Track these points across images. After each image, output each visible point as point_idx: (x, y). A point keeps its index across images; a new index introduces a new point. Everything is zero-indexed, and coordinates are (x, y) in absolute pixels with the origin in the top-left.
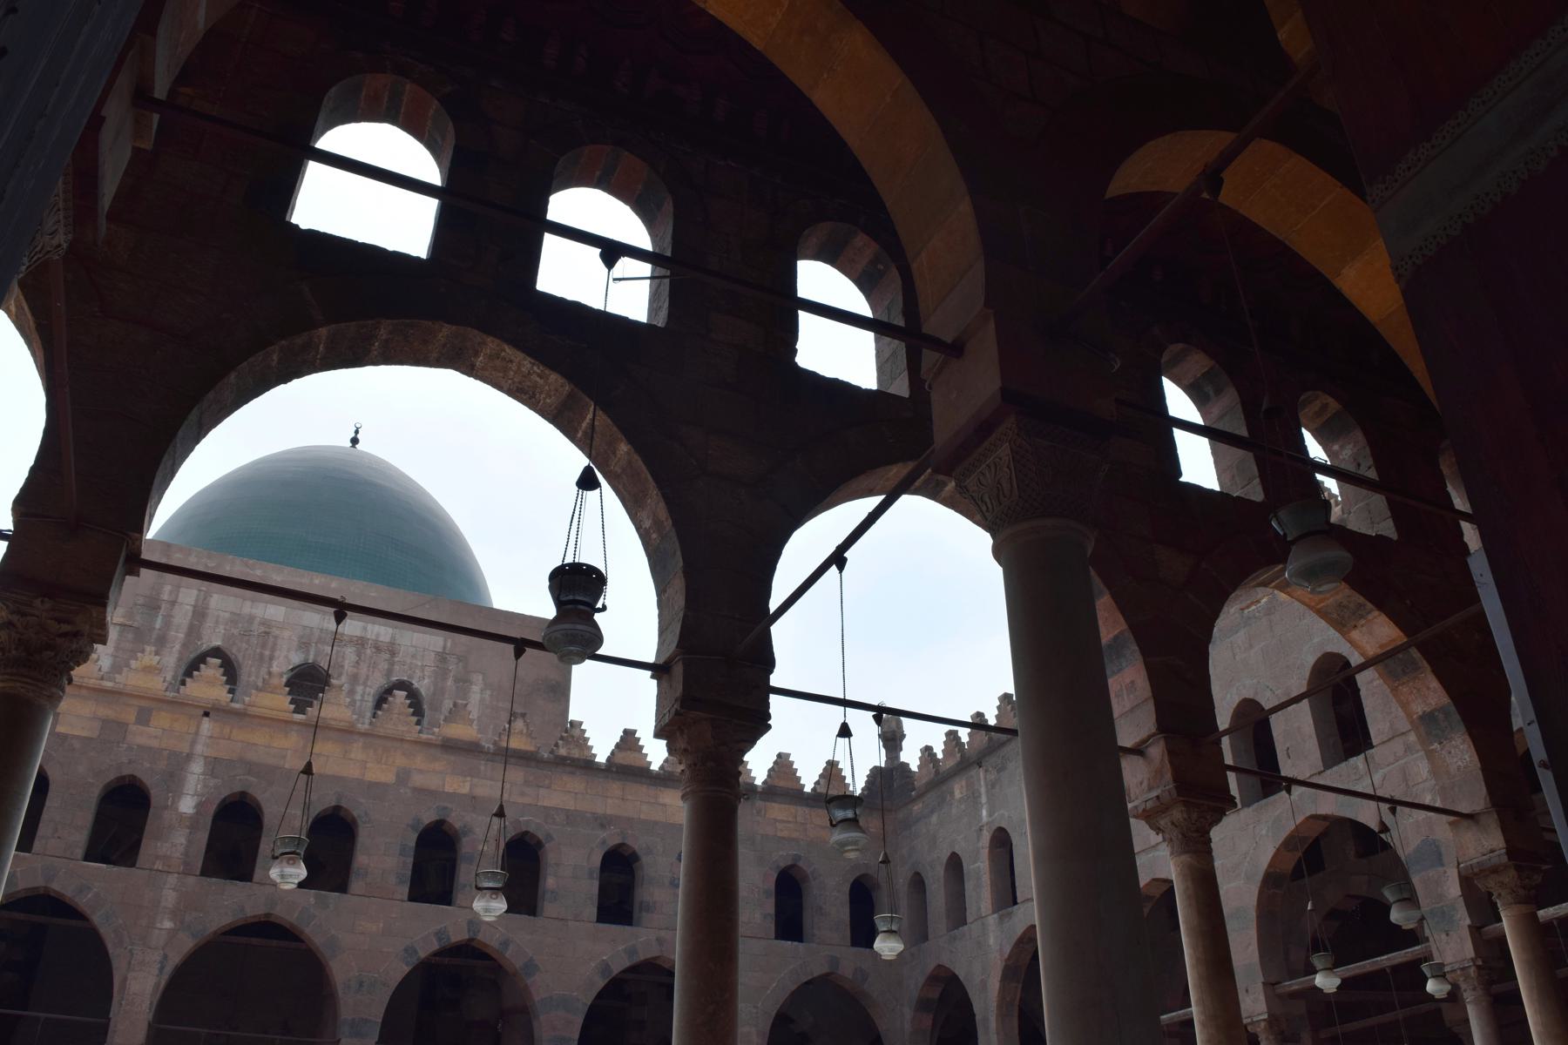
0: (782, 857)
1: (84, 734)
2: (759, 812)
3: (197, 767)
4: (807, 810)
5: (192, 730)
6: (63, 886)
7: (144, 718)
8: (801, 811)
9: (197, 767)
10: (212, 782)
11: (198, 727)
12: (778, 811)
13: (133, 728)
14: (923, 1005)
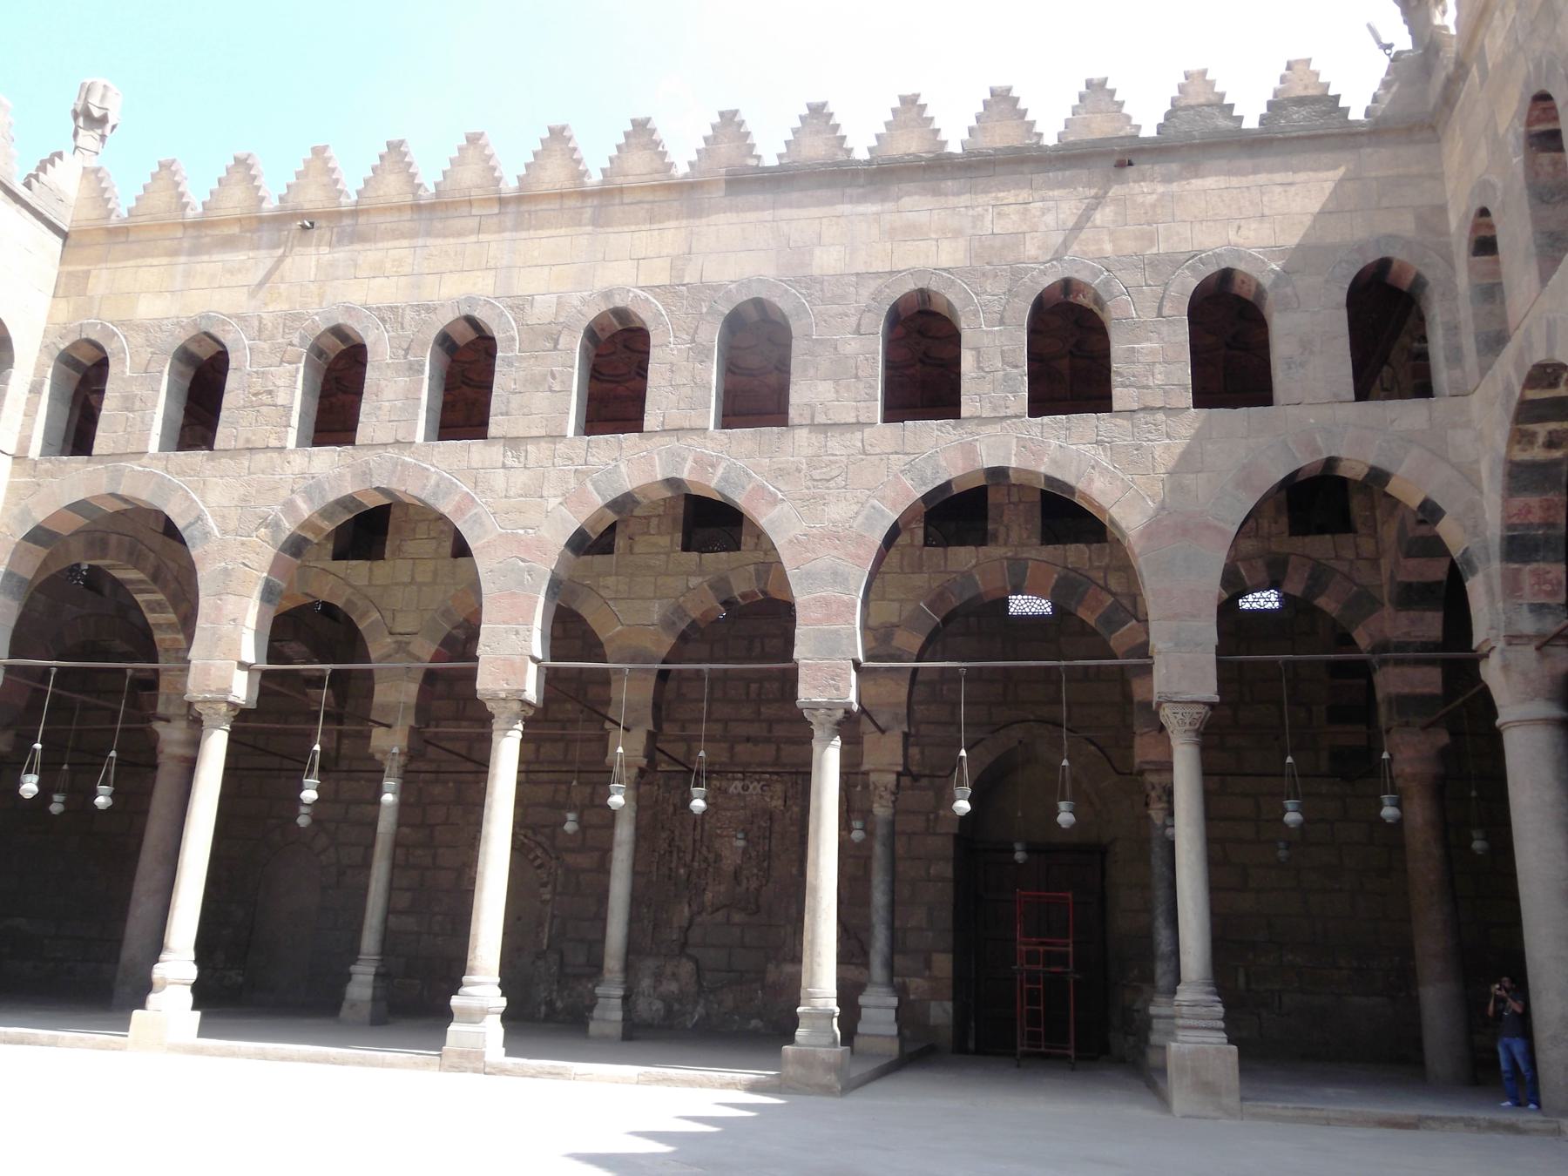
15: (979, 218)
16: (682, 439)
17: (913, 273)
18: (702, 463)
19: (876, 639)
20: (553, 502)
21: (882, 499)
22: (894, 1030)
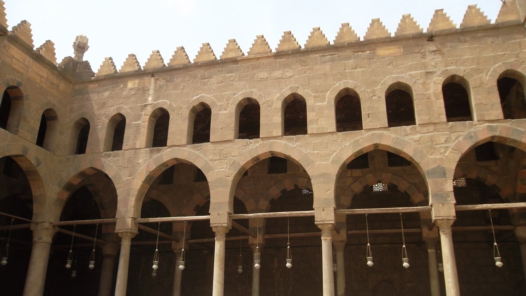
0: (12, 79)
2: (5, 47)
4: (31, 60)
8: (29, 60)
12: (15, 52)
14: (68, 187)
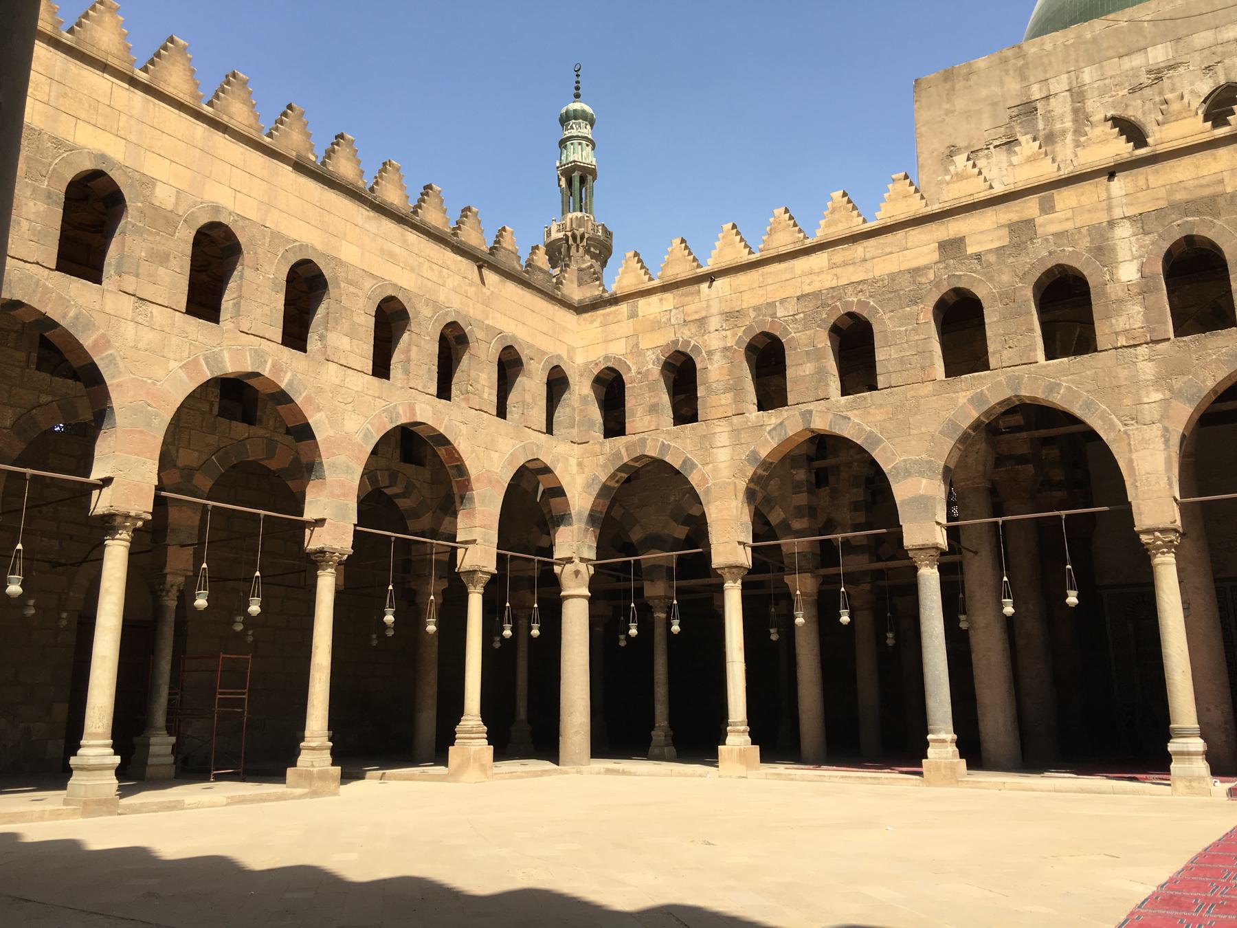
1: (997, 245)
3: (1124, 232)
5: (1104, 196)
6: (1032, 390)
7: (1047, 208)
9: (1124, 232)
10: (1148, 239)
11: (1108, 190)
13: (1039, 220)
15: (420, 265)
16: (246, 338)
17: (395, 285)
18: (277, 368)
19: (182, 477)
20: (173, 365)
21: (373, 425)
22: (171, 759)
